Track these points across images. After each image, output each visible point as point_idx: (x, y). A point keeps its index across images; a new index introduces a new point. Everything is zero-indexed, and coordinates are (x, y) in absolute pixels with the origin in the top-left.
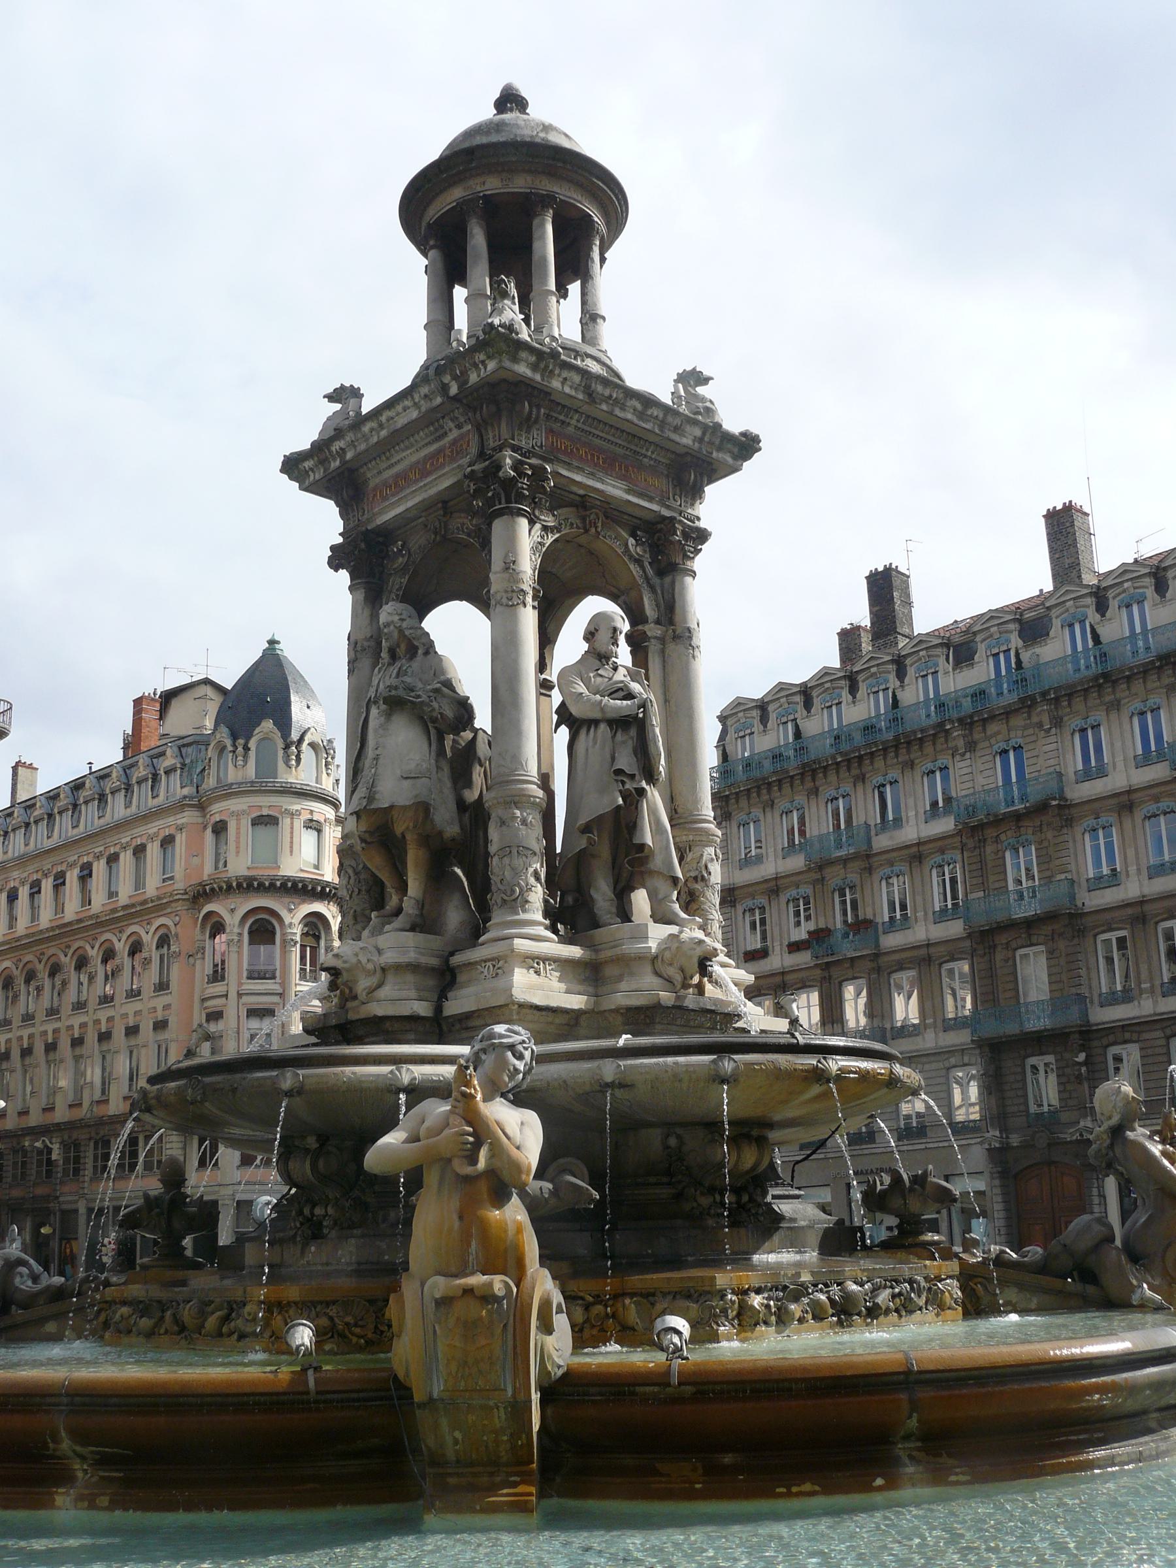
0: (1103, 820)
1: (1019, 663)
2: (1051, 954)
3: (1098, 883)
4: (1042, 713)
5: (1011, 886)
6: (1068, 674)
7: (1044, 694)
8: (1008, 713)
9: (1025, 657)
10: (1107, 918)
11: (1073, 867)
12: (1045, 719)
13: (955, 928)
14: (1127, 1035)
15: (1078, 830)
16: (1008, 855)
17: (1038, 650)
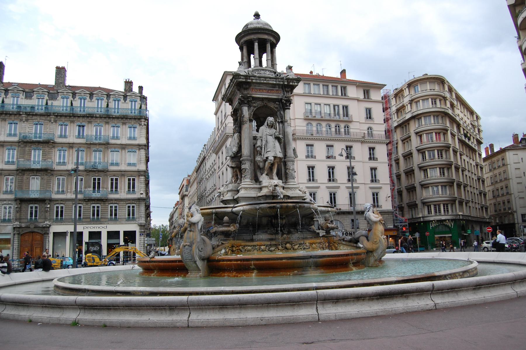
0: (64, 149)
1: (47, 103)
2: (42, 179)
3: (59, 164)
4: (53, 118)
5: (32, 159)
6: (61, 110)
7: (54, 113)
8: (41, 115)
9: (50, 103)
10: (61, 173)
11: (53, 158)
12: (52, 120)
13: (13, 167)
14: (62, 202)
15: (56, 149)
16: (33, 151)
17: (53, 102)
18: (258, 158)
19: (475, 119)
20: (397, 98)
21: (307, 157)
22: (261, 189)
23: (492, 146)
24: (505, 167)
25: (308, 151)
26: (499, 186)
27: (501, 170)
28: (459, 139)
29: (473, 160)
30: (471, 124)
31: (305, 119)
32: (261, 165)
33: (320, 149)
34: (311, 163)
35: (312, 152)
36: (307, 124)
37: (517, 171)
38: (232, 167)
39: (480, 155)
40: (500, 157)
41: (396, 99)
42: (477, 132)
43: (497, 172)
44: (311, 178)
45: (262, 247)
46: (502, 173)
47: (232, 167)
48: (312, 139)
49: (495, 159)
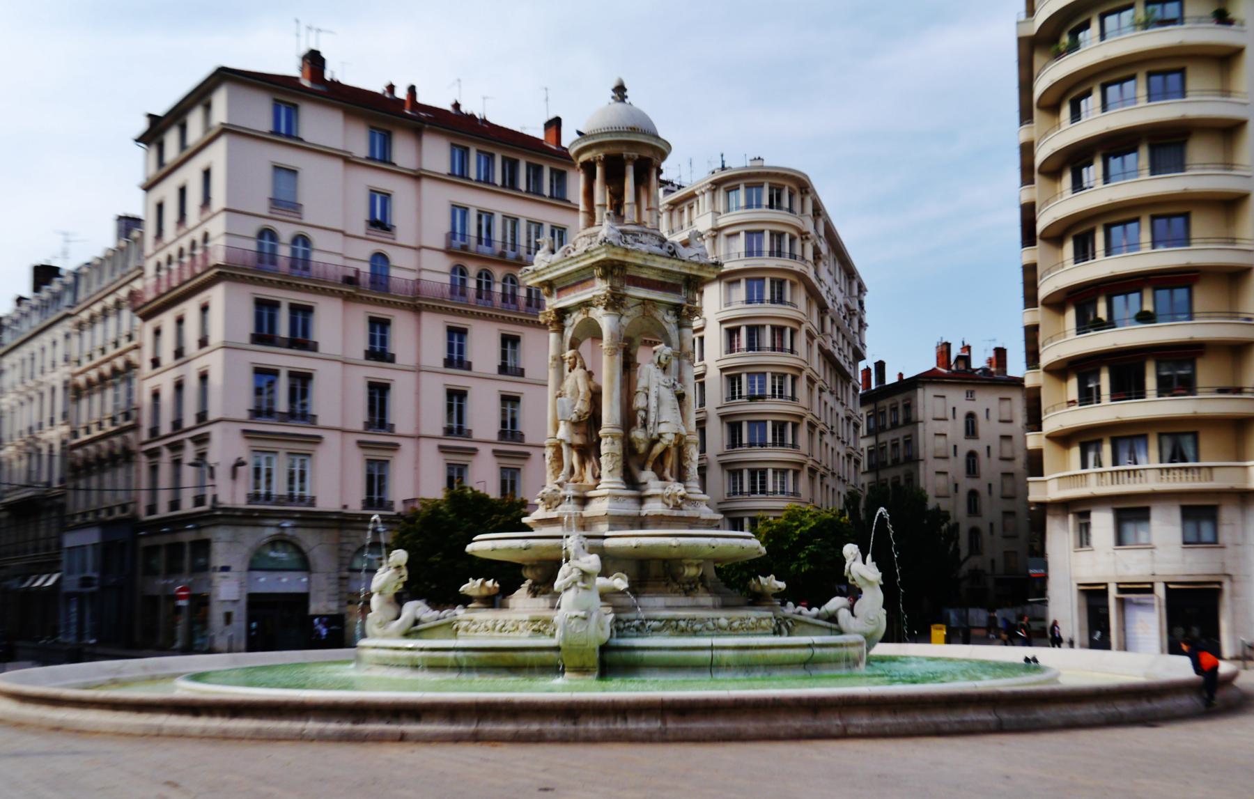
18: (638, 434)
19: (856, 292)
20: (676, 214)
21: (449, 363)
22: (641, 500)
23: (880, 366)
24: (910, 427)
25: (450, 348)
26: (887, 475)
27: (900, 434)
28: (820, 347)
29: (842, 404)
30: (846, 306)
31: (449, 251)
32: (642, 448)
33: (483, 343)
34: (457, 380)
35: (461, 349)
36: (454, 270)
37: (941, 440)
38: (570, 446)
39: (856, 390)
40: (899, 399)
41: (671, 217)
42: (856, 329)
43: (886, 437)
44: (455, 425)
46: (901, 443)
47: (570, 446)
48: (466, 314)
49: (886, 403)
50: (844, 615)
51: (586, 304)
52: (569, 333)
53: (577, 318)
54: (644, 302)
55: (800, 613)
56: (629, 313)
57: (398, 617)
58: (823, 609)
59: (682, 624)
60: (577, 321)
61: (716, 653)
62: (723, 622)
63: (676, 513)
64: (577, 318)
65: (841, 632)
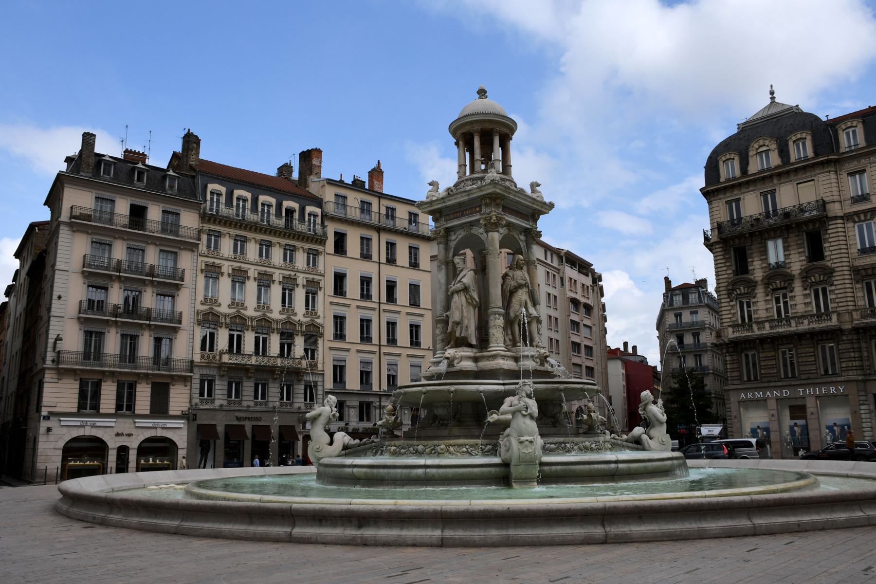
45: (568, 445)
50: (645, 437)
51: (472, 224)
52: (453, 244)
53: (461, 234)
54: (509, 225)
55: (614, 438)
56: (501, 231)
57: (331, 443)
58: (630, 435)
59: (568, 445)
60: (460, 237)
61: (621, 466)
62: (587, 444)
63: (542, 368)
64: (461, 234)
65: (644, 449)
